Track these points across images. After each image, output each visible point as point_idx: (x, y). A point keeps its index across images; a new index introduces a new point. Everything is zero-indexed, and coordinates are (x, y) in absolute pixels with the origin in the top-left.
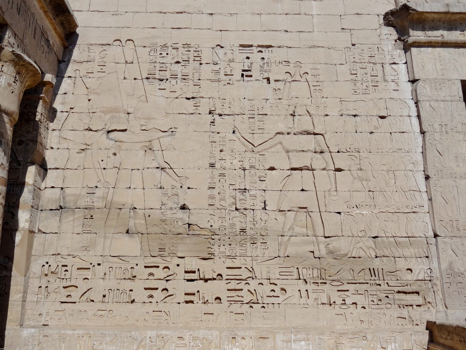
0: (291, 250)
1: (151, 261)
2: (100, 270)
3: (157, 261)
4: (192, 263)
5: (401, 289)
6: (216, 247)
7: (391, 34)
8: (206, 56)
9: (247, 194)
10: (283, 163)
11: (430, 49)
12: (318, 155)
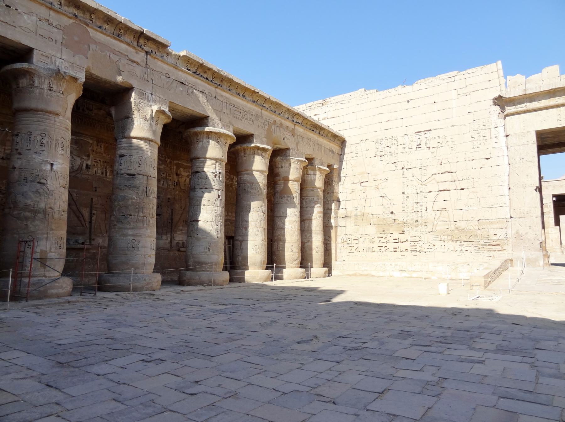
0: (438, 228)
1: (380, 236)
2: (361, 240)
3: (382, 235)
4: (396, 236)
5: (490, 244)
6: (405, 228)
7: (498, 109)
8: (400, 141)
9: (419, 204)
10: (435, 188)
11: (518, 116)
12: (453, 183)
